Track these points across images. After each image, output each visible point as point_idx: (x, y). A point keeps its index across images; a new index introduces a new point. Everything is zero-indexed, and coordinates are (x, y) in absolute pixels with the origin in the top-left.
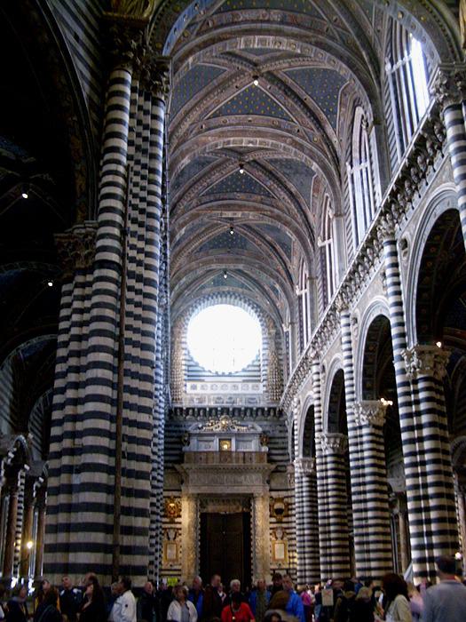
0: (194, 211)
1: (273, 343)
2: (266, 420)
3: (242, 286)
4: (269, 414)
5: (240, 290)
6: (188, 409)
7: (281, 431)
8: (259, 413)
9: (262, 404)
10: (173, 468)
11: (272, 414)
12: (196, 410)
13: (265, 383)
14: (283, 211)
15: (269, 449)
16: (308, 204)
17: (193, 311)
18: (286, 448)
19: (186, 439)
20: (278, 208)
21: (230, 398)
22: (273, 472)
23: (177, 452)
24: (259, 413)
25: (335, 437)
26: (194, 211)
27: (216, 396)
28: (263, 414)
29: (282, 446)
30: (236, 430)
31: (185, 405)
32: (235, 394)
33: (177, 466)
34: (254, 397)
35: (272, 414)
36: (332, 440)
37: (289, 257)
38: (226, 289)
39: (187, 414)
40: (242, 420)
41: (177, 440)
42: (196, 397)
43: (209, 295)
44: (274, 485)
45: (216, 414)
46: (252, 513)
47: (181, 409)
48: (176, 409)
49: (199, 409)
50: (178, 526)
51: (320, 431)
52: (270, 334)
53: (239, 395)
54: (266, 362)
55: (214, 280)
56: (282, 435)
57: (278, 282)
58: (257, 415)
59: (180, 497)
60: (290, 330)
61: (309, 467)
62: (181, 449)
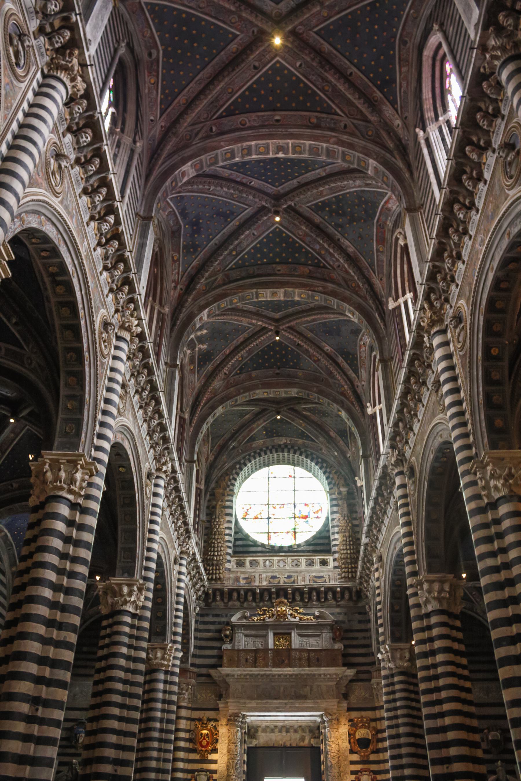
0: (219, 291)
1: (345, 505)
2: (338, 606)
3: (302, 435)
4: (343, 597)
5: (300, 441)
6: (231, 591)
7: (360, 622)
8: (330, 595)
9: (332, 583)
10: (209, 676)
11: (347, 596)
12: (242, 592)
13: (337, 556)
14: (339, 285)
15: (346, 647)
16: (371, 265)
17: (241, 469)
18: (369, 646)
19: (228, 633)
20: (333, 281)
21: (289, 577)
22: (351, 681)
23: (214, 652)
24: (330, 595)
25: (442, 582)
26: (219, 291)
27: (270, 575)
28: (334, 597)
29: (362, 642)
30: (297, 619)
31: (228, 584)
32: (296, 572)
33: (212, 671)
34: (321, 574)
35: (347, 596)
36: (436, 586)
37: (356, 371)
38: (283, 441)
39: (230, 598)
40: (305, 607)
41: (216, 635)
42: (242, 576)
43: (261, 450)
44: (354, 700)
45: (270, 599)
46: (322, 746)
47: (221, 591)
48: (215, 590)
49: (247, 591)
50: (213, 767)
51: (414, 574)
52: (340, 493)
53: (301, 572)
54: (336, 529)
55: (265, 428)
56: (363, 626)
57: (343, 407)
58: (326, 599)
59: (216, 720)
60: (363, 483)
61: (402, 658)
62: (220, 648)
